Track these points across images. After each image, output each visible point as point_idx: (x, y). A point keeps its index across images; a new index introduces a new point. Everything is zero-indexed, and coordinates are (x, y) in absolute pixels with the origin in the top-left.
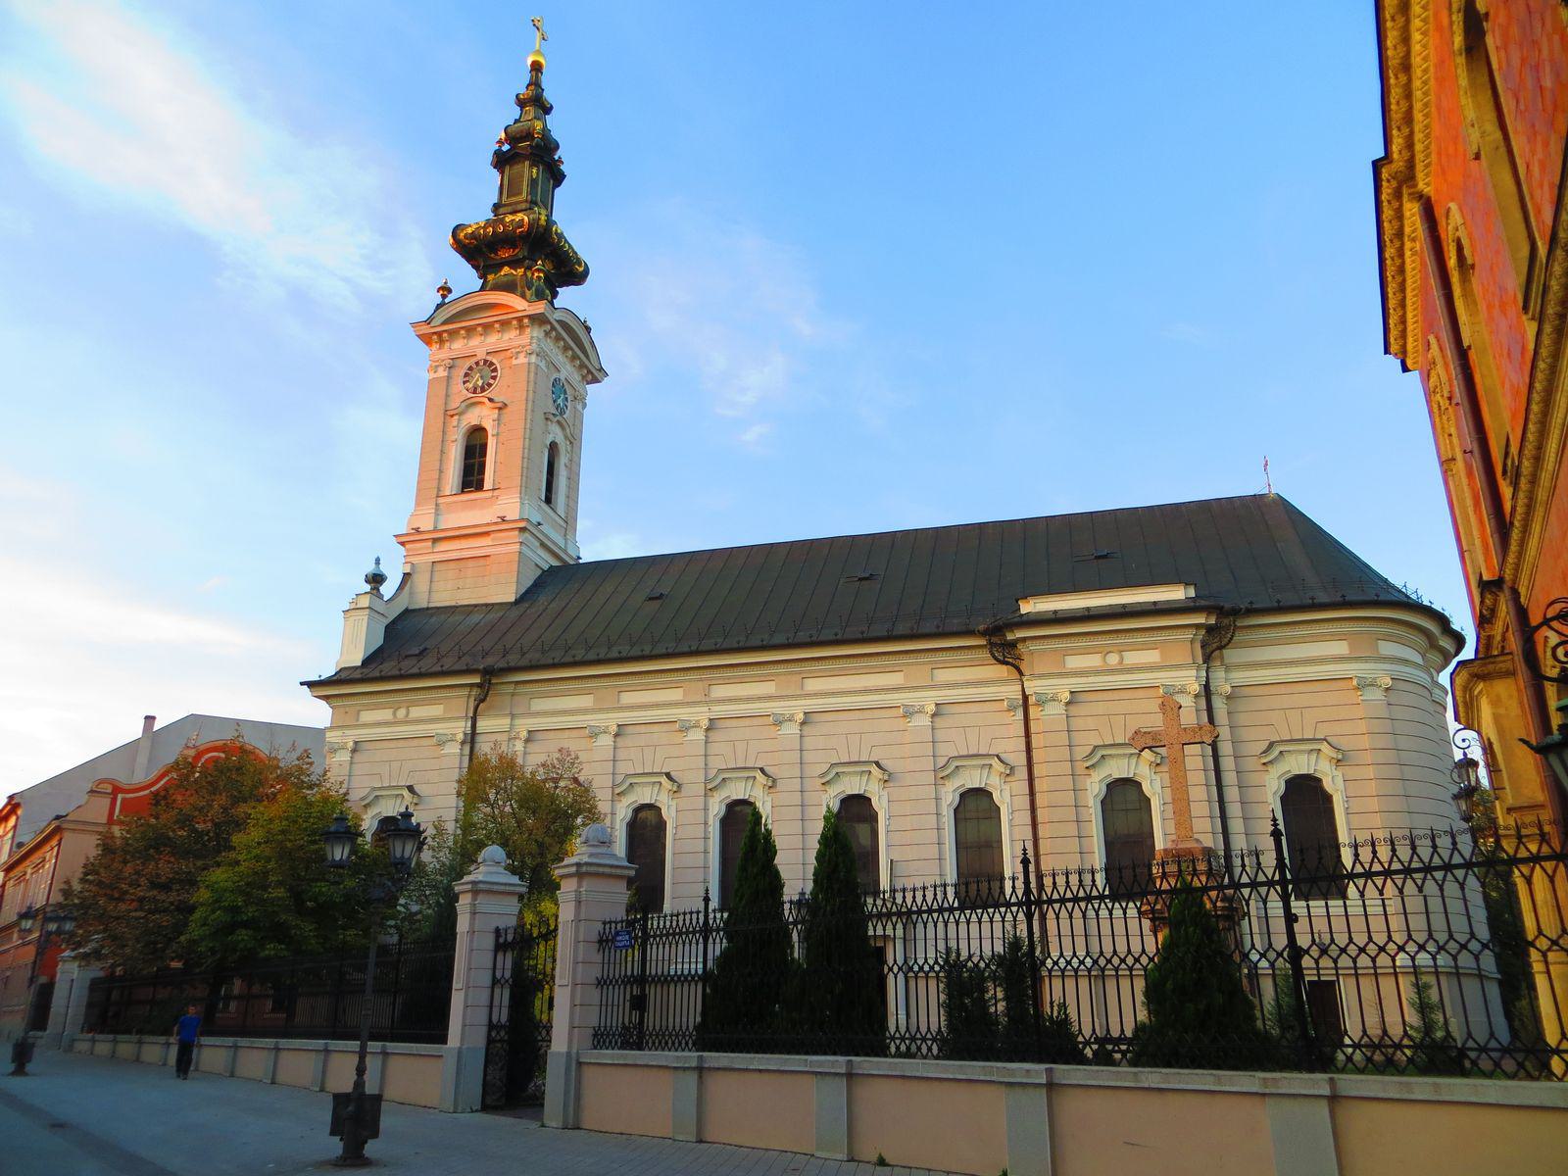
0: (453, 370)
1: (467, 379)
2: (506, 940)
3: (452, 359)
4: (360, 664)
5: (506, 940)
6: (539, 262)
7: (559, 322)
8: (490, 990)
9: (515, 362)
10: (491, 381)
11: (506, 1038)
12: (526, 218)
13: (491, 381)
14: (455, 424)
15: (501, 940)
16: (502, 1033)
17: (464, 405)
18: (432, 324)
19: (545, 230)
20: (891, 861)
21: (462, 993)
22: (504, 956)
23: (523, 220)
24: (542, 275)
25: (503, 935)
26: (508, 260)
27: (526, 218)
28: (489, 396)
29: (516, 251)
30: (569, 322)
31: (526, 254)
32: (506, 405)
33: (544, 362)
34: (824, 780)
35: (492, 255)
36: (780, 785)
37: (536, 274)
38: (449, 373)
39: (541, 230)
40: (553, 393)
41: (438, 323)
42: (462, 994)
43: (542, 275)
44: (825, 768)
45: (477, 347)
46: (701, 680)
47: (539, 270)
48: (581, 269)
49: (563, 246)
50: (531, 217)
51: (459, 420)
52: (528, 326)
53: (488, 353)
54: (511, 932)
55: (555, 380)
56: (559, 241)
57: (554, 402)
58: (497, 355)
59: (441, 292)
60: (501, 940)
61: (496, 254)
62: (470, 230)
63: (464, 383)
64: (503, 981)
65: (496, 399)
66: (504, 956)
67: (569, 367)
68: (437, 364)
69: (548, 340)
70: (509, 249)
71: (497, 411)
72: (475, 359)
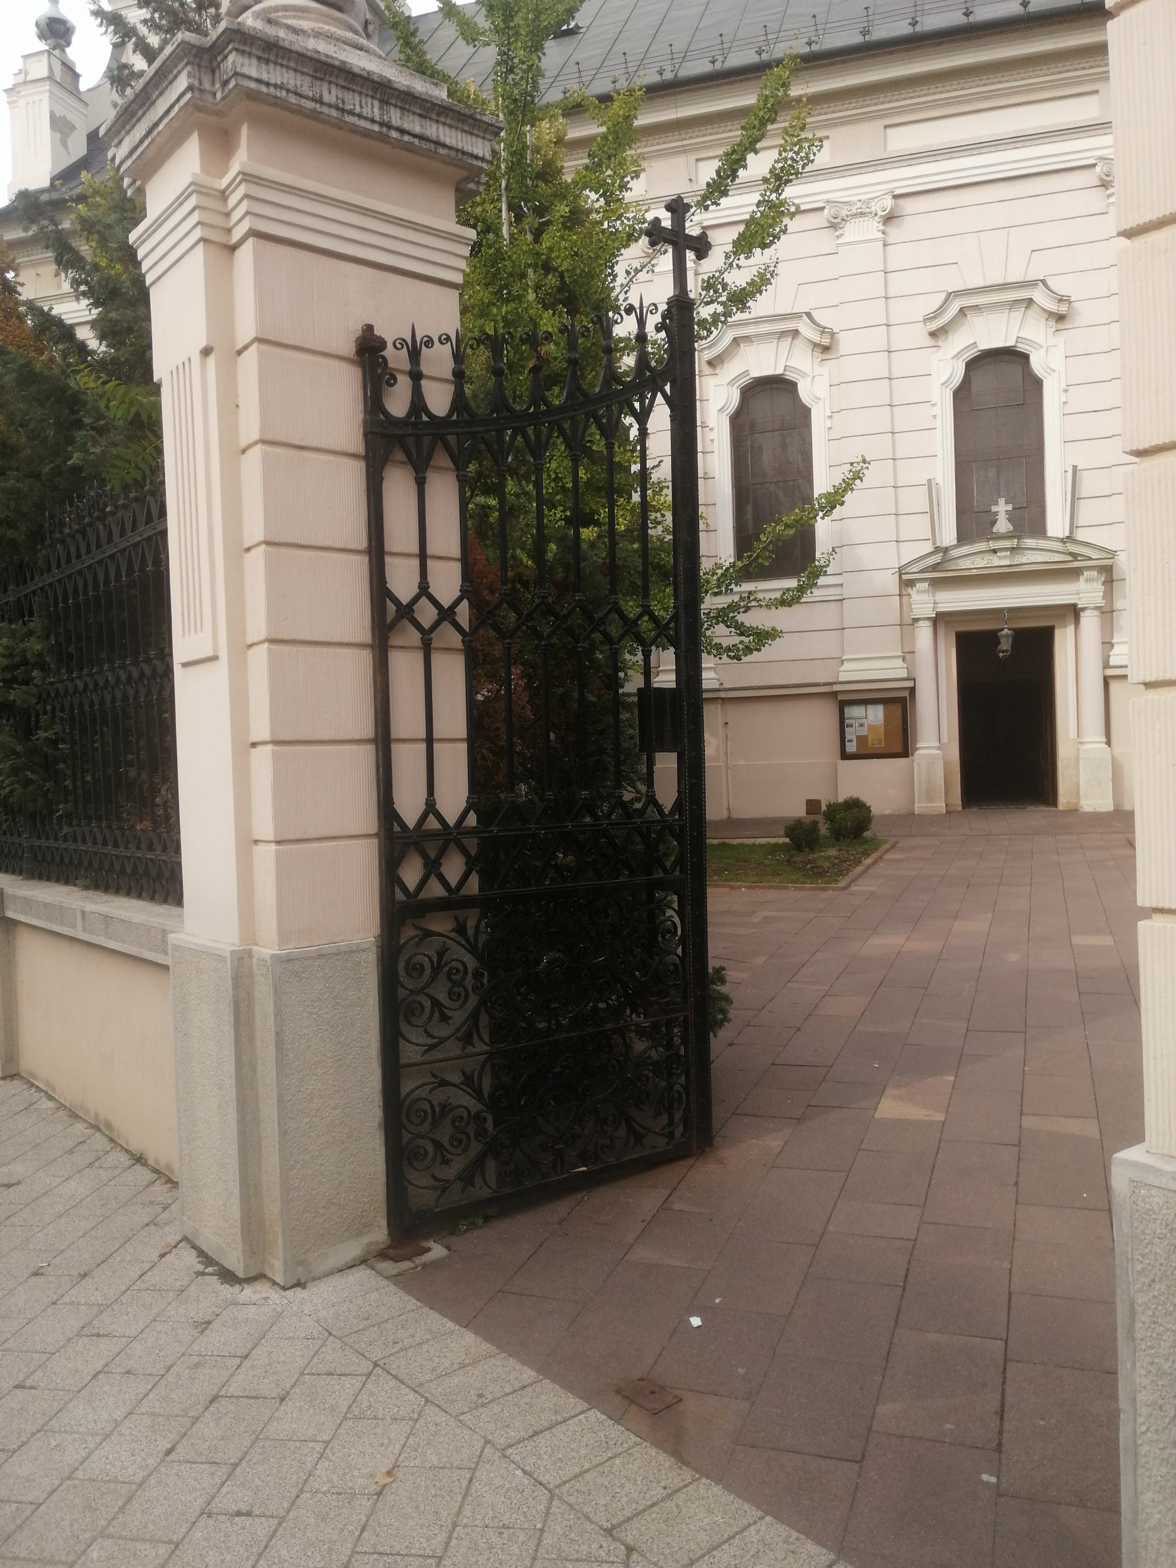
2: (418, 404)
4: (46, 183)
5: (418, 404)
8: (363, 660)
11: (473, 885)
15: (398, 404)
16: (453, 869)
20: (1075, 468)
21: (219, 673)
22: (421, 483)
25: (404, 384)
34: (934, 326)
36: (845, 343)
42: (218, 676)
44: (936, 302)
46: (684, 151)
54: (438, 361)
60: (398, 404)
64: (426, 614)
66: (421, 483)
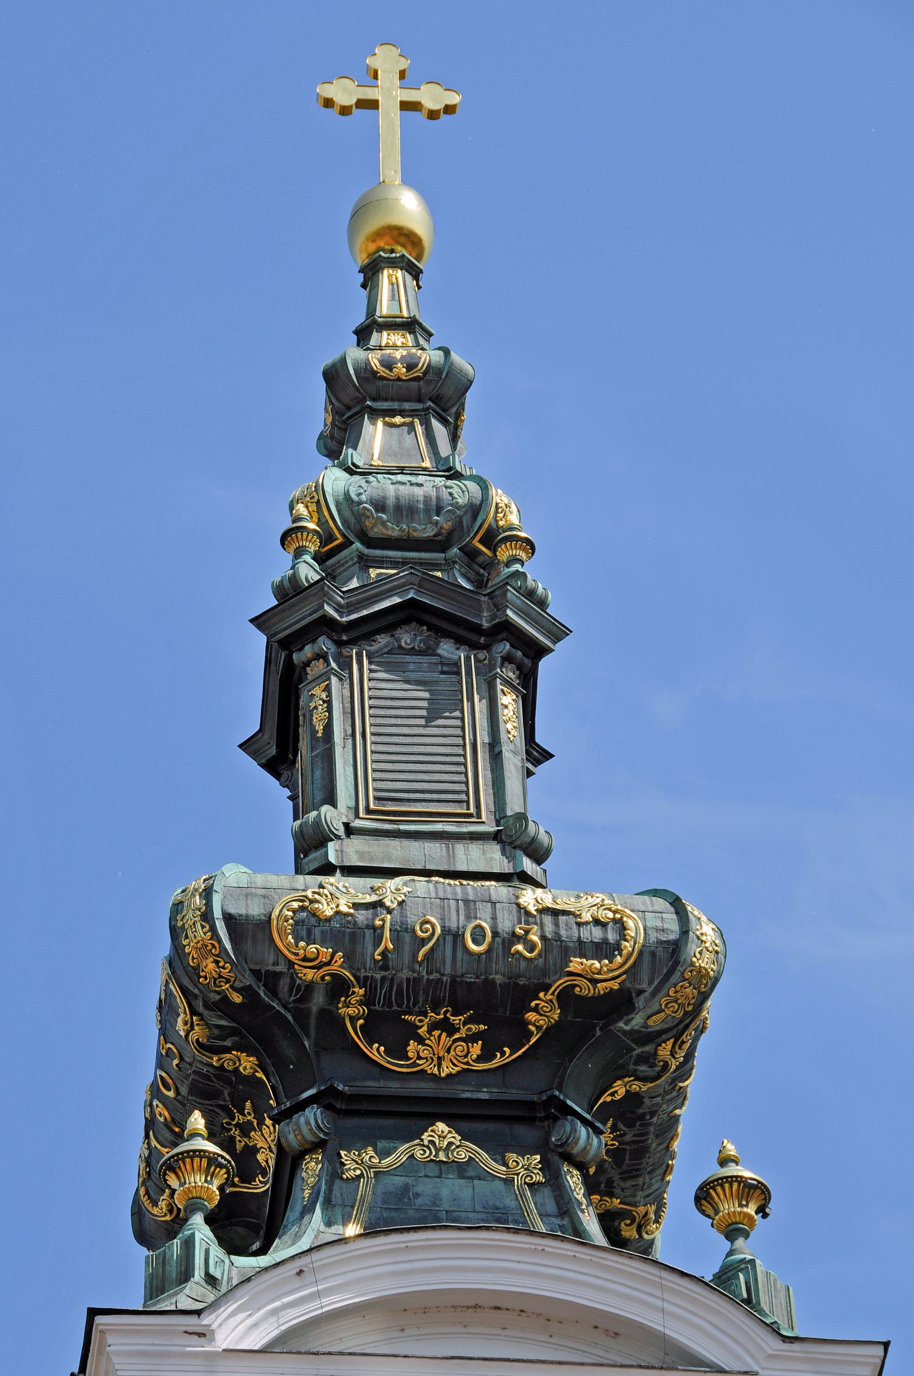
29: (497, 1061)
35: (376, 1052)
70: (471, 1039)
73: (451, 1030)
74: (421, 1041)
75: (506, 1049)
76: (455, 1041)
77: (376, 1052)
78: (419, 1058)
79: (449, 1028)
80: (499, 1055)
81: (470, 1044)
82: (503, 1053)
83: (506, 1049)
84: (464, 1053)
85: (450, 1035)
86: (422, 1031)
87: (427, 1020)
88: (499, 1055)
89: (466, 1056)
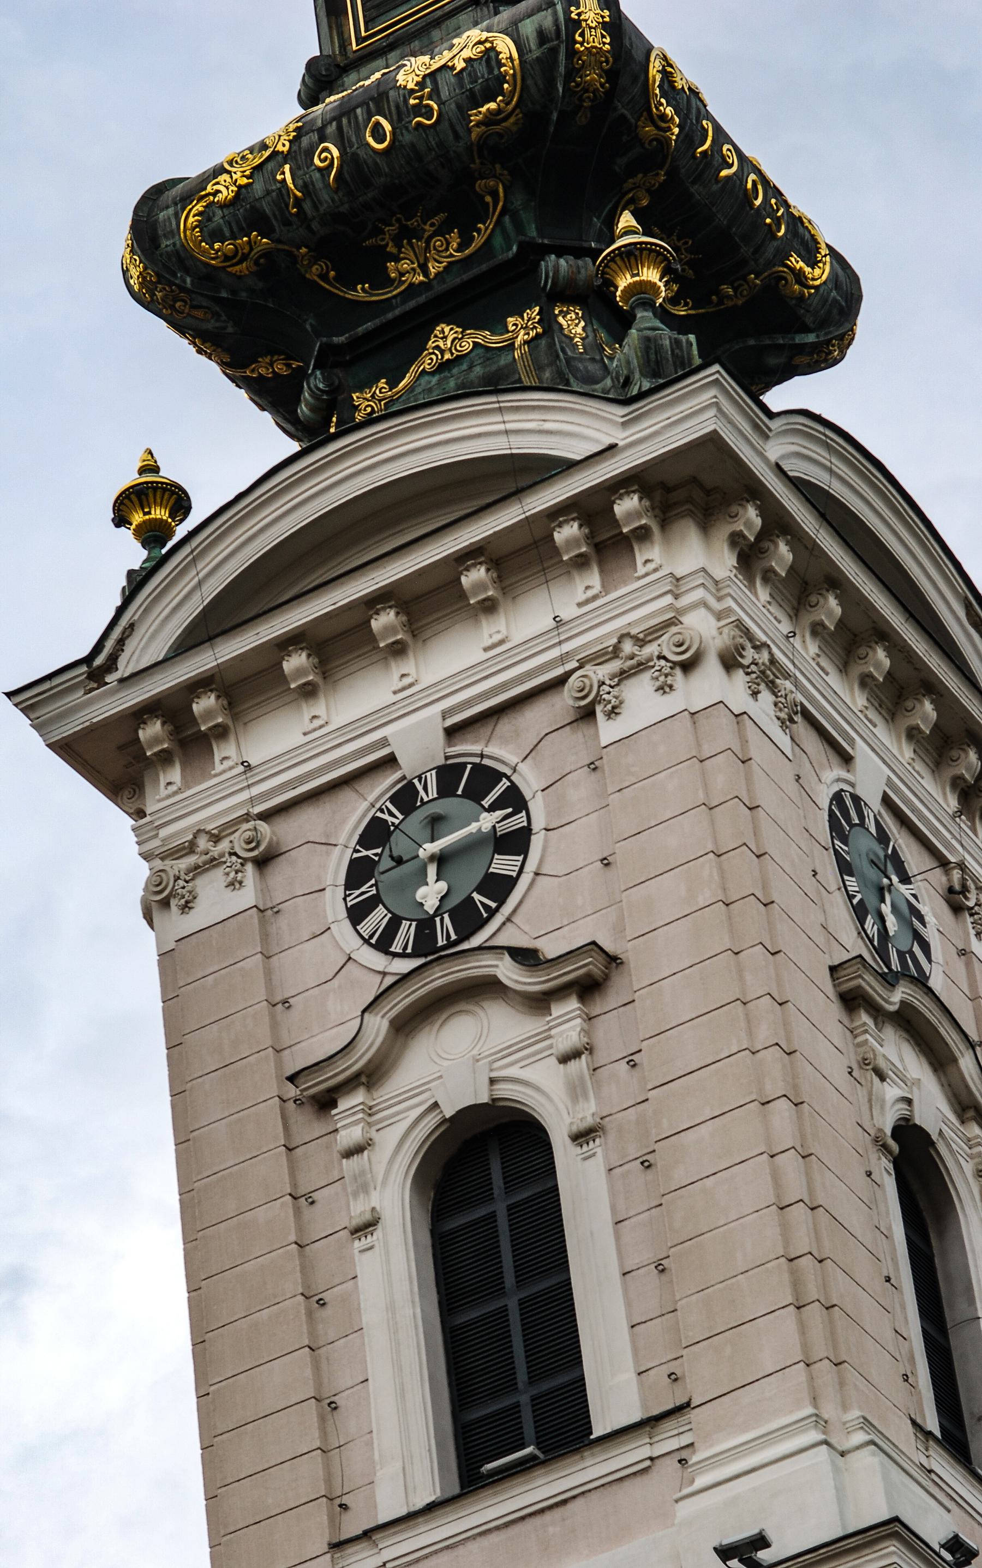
0: (280, 873)
1: (368, 889)
3: (266, 816)
6: (626, 220)
7: (800, 486)
9: (608, 730)
10: (503, 864)
12: (505, 46)
13: (503, 864)
14: (351, 1135)
17: (378, 1025)
18: (125, 667)
19: (612, 75)
23: (490, 56)
24: (651, 275)
26: (438, 288)
27: (505, 46)
28: (512, 937)
29: (478, 241)
30: (837, 489)
31: (532, 232)
32: (613, 960)
33: (766, 697)
35: (360, 293)
37: (624, 281)
38: (264, 890)
39: (592, 76)
40: (845, 868)
41: (158, 650)
43: (651, 275)
45: (385, 717)
47: (631, 257)
48: (820, 274)
49: (715, 160)
50: (528, 28)
51: (370, 1111)
52: (643, 534)
53: (452, 733)
55: (838, 798)
56: (692, 134)
57: (860, 912)
58: (505, 726)
59: (138, 518)
61: (381, 280)
62: (224, 190)
63: (357, 914)
65: (551, 948)
67: (882, 732)
68: (192, 860)
69: (763, 594)
70: (442, 231)
71: (572, 1005)
72: (386, 783)
73: (415, 233)
74: (397, 260)
75: (480, 225)
76: (428, 242)
77: (360, 293)
78: (402, 274)
79: (406, 235)
80: (475, 234)
81: (447, 236)
82: (479, 231)
83: (480, 225)
84: (444, 247)
85: (419, 239)
86: (391, 249)
87: (387, 236)
88: (475, 234)
89: (447, 249)
